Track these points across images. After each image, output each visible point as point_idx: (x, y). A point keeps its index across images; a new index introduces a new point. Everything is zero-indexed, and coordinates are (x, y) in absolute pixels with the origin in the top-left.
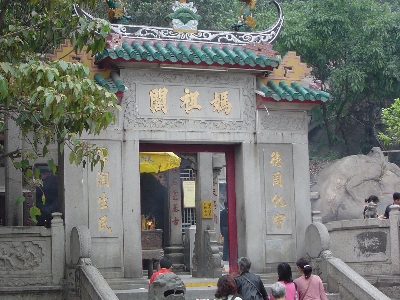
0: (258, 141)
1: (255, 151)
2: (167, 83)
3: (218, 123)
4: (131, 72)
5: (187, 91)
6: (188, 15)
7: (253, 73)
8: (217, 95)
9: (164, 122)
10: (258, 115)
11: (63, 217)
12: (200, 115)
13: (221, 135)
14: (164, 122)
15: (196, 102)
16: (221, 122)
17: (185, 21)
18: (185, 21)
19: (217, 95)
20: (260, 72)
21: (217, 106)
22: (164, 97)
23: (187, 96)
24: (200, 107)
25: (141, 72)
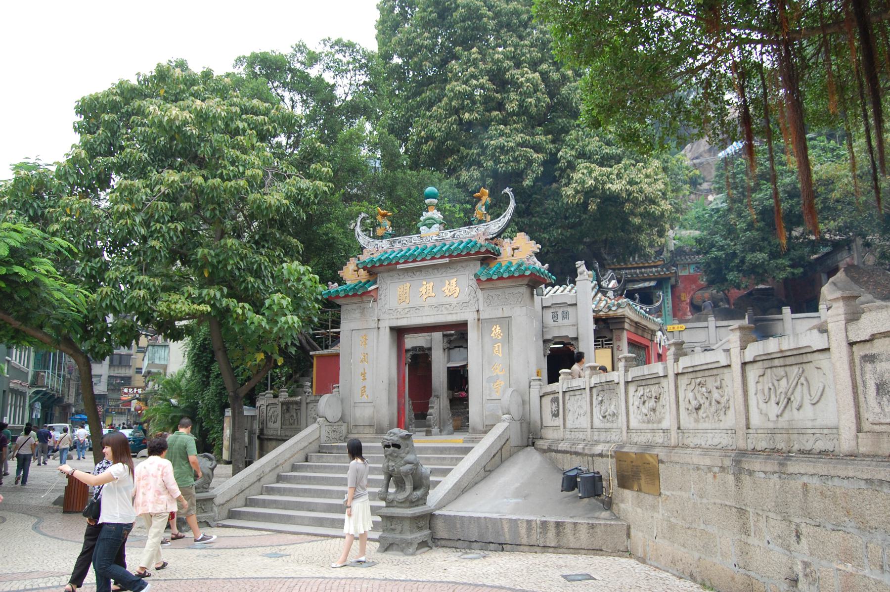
0: (481, 317)
1: (478, 326)
2: (410, 279)
4: (385, 275)
5: (424, 283)
7: (478, 259)
10: (480, 294)
12: (433, 301)
17: (429, 226)
18: (429, 226)
20: (488, 257)
21: (447, 291)
25: (391, 274)
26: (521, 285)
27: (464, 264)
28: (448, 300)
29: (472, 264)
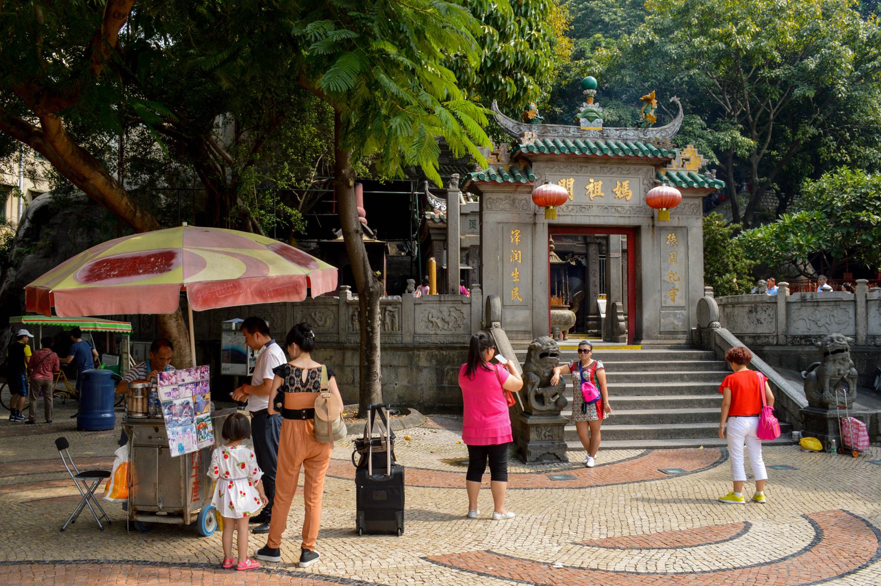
3: (619, 209)
4: (542, 165)
5: (592, 180)
6: (594, 115)
8: (619, 184)
9: (570, 208)
11: (481, 288)
12: (602, 201)
13: (622, 219)
14: (570, 208)
15: (599, 190)
16: (622, 207)
17: (591, 119)
19: (619, 184)
21: (618, 193)
22: (571, 186)
23: (592, 185)
24: (603, 194)
26: (698, 197)
27: (638, 167)
28: (617, 202)
29: (645, 168)
